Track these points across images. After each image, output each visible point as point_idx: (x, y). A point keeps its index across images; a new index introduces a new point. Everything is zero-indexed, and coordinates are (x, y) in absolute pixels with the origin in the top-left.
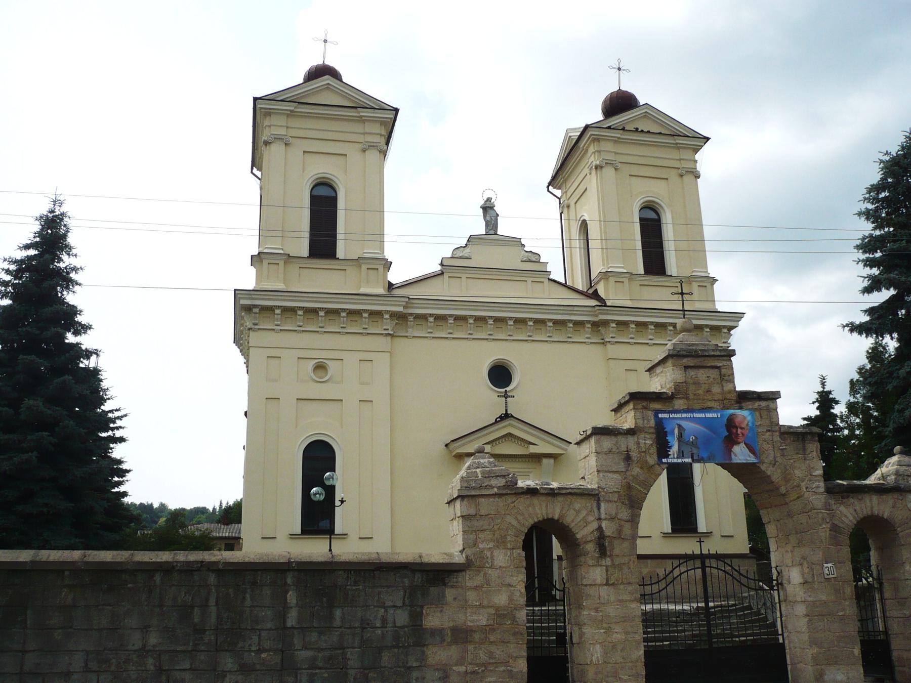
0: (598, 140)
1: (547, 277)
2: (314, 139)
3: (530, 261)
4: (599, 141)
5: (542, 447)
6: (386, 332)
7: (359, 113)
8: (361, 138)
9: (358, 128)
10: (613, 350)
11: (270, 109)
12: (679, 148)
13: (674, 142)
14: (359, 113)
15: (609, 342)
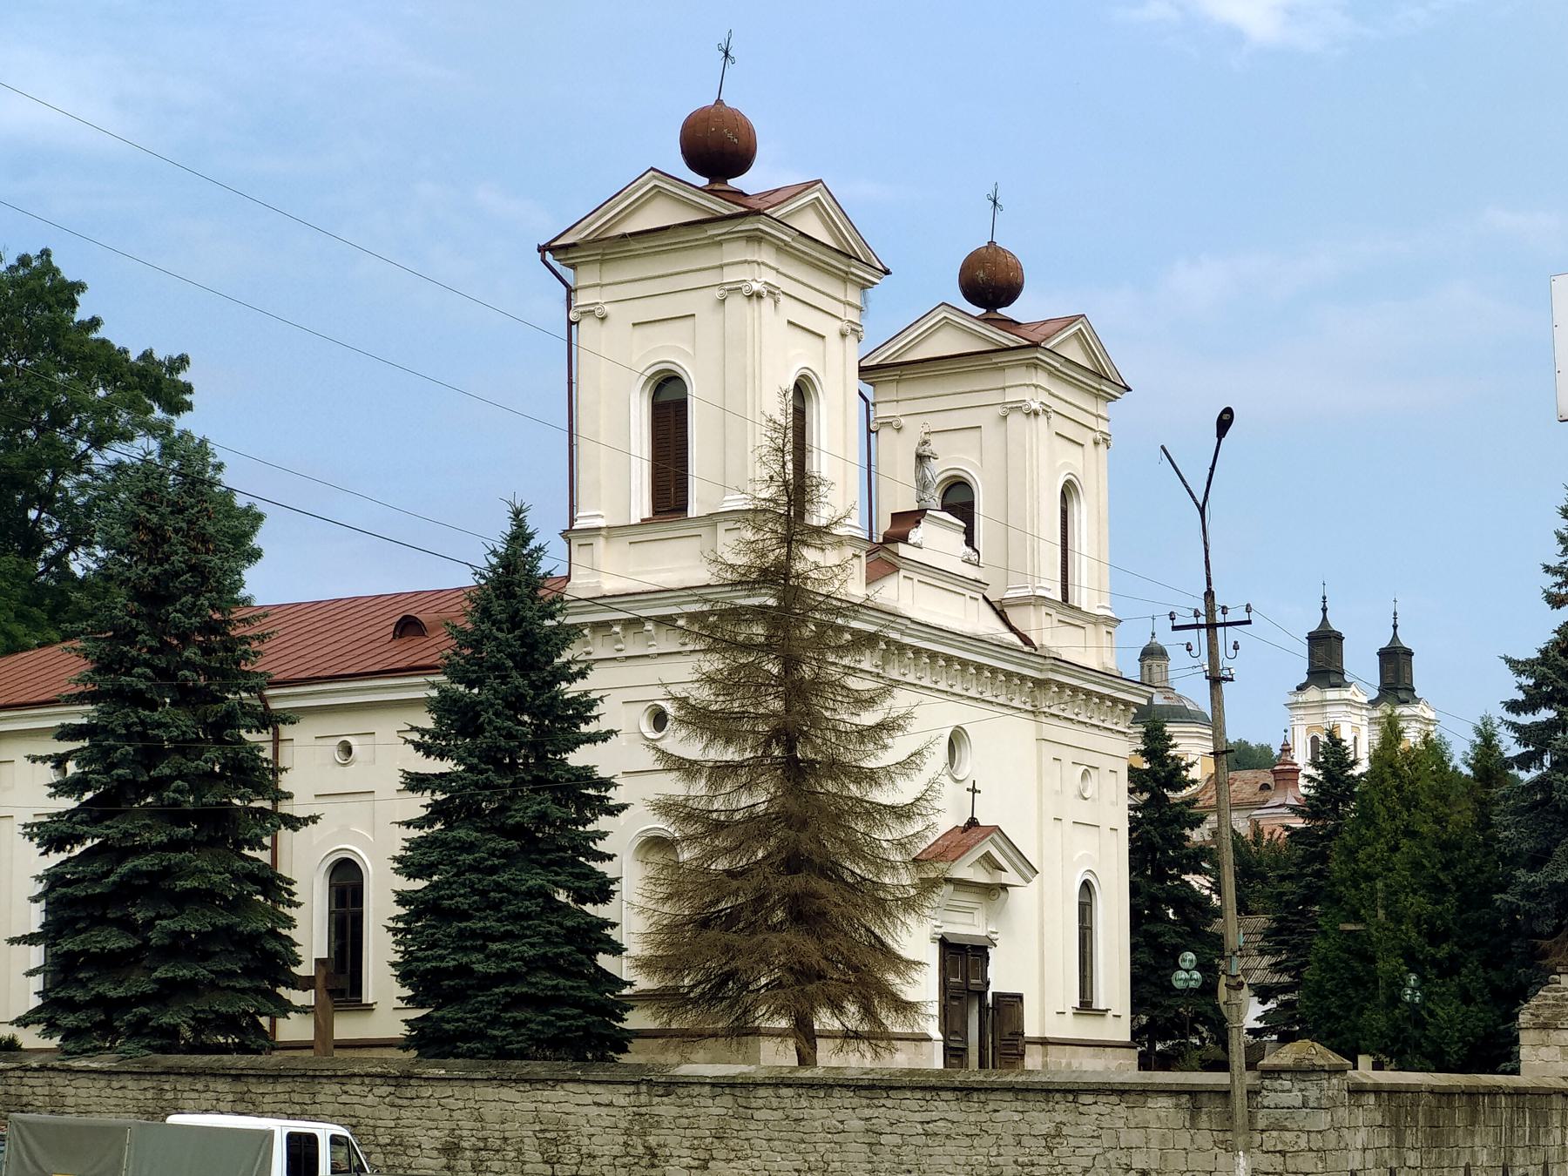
0: (1036, 366)
1: (982, 591)
2: (811, 305)
3: (968, 561)
4: (1036, 368)
5: (1009, 877)
6: (876, 670)
7: (849, 266)
8: (838, 309)
9: (834, 288)
10: (1055, 730)
11: (767, 233)
12: (1097, 396)
13: (1097, 386)
14: (849, 266)
15: (1044, 713)
